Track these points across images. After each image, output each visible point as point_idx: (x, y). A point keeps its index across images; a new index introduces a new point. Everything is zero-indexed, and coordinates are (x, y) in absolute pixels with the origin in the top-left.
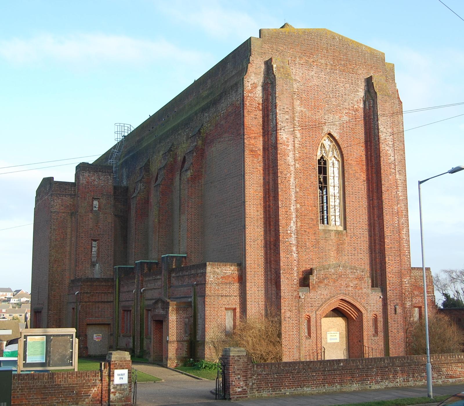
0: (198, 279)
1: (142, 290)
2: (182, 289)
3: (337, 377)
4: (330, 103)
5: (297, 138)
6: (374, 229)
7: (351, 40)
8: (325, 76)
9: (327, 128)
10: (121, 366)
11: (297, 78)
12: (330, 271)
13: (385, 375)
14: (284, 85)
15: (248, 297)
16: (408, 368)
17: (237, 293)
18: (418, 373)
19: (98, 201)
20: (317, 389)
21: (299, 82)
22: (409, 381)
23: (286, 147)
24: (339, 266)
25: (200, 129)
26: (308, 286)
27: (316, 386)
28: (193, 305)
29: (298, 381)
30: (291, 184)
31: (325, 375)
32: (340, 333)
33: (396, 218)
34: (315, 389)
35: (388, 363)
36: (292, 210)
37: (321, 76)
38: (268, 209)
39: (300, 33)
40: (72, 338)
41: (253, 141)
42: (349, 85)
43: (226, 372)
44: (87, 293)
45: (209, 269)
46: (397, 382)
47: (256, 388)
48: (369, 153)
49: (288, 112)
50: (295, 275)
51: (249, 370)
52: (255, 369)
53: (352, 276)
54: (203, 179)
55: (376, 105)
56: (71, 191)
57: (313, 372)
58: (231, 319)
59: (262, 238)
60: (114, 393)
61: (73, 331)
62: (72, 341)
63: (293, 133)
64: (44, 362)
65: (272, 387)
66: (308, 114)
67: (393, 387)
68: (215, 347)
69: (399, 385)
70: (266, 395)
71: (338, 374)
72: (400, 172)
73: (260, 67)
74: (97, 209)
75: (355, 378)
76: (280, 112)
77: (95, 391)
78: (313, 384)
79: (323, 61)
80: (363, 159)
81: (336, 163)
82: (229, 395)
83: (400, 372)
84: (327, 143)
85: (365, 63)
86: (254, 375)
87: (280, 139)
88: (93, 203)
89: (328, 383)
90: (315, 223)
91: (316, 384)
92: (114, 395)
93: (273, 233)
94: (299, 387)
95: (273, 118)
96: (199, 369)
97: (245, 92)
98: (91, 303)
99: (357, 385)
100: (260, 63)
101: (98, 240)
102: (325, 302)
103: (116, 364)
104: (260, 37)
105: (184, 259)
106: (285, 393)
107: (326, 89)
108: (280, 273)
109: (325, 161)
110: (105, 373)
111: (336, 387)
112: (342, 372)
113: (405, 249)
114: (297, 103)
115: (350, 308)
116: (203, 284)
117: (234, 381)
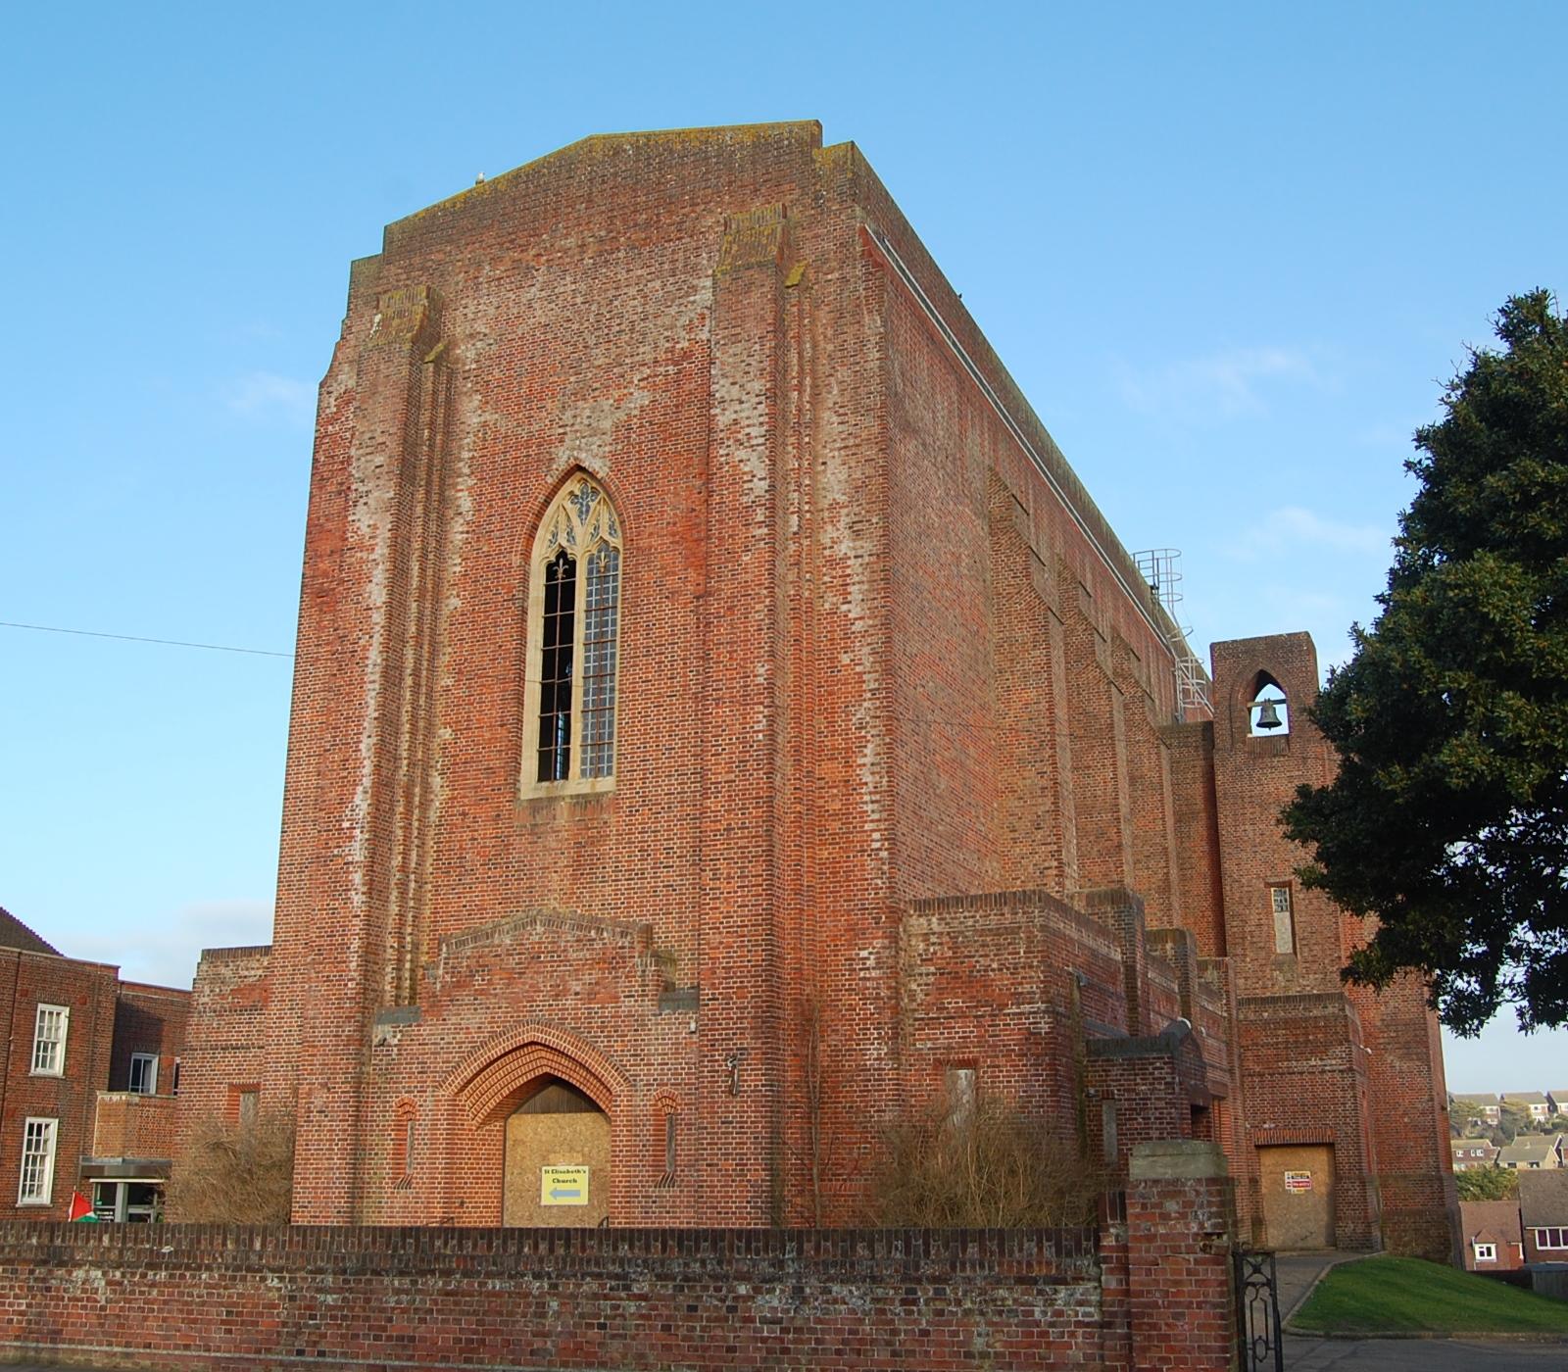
5: (460, 514)
8: (573, 287)
9: (568, 452)
12: (496, 942)
21: (485, 335)
23: (364, 555)
24: (534, 922)
32: (593, 1174)
36: (364, 750)
42: (659, 282)
49: (384, 443)
66: (505, 426)
76: (361, 451)
79: (571, 242)
80: (698, 521)
90: (499, 781)
113: (867, 827)
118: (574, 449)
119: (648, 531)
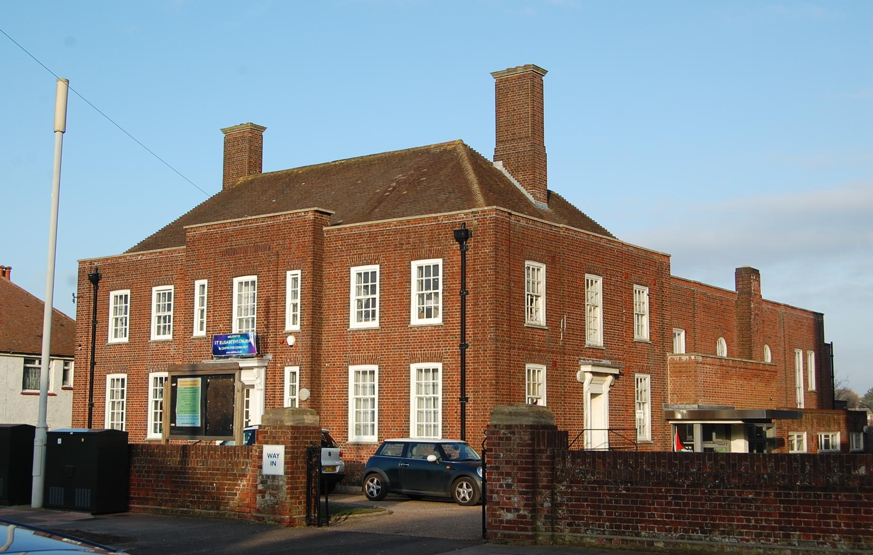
3: (835, 511)
10: (274, 438)
20: (759, 544)
27: (758, 535)
29: (694, 511)
31: (789, 502)
34: (752, 542)
47: (567, 518)
52: (569, 465)
57: (744, 487)
65: (611, 521)
70: (593, 541)
71: (842, 504)
77: (244, 486)
78: (743, 527)
86: (560, 482)
92: (263, 497)
106: (651, 544)
111: (834, 546)
112: (860, 497)
117: (497, 493)
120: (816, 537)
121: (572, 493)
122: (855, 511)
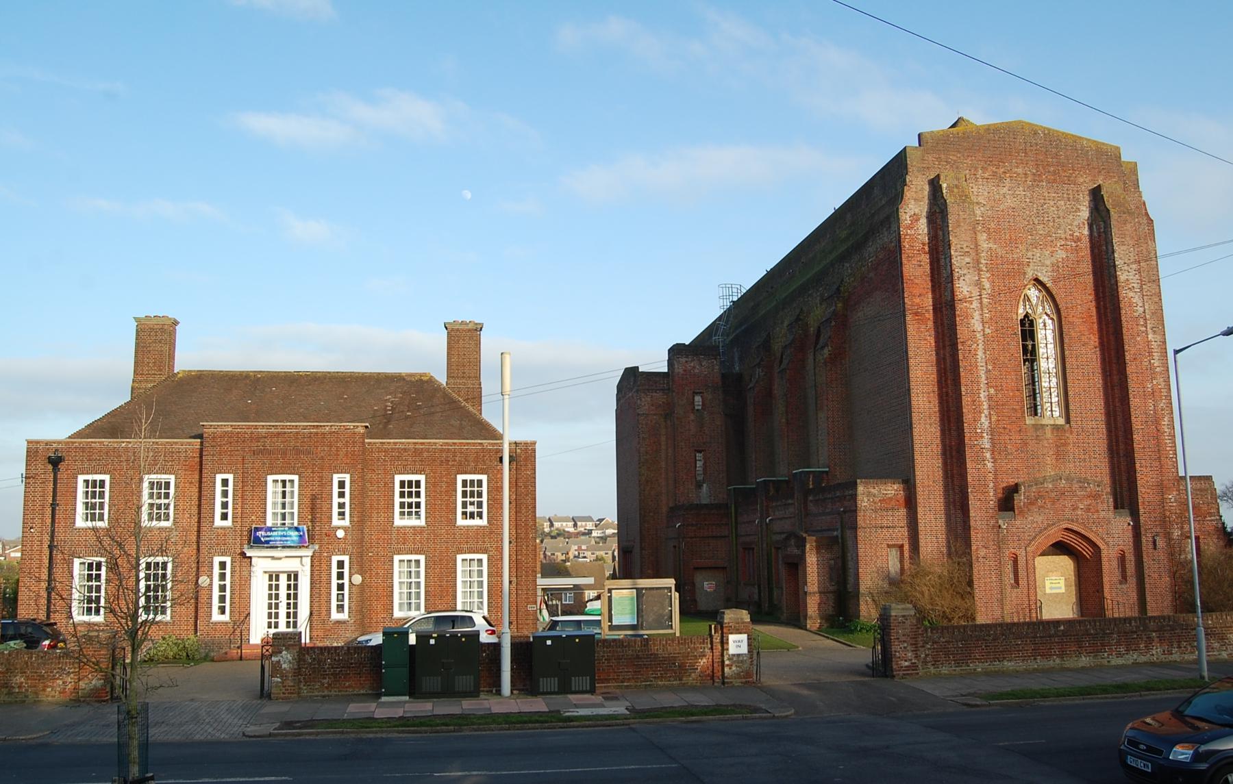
0: (846, 503)
1: (768, 520)
2: (824, 517)
4: (1034, 232)
5: (985, 289)
6: (1115, 420)
7: (1063, 133)
8: (1024, 193)
10: (738, 630)
11: (981, 200)
12: (1046, 486)
13: (1133, 644)
14: (961, 213)
15: (921, 527)
16: (1171, 634)
17: (904, 523)
18: (1187, 641)
19: (701, 396)
22: (1172, 654)
23: (967, 305)
24: (1061, 479)
25: (840, 286)
26: (1012, 509)
27: (1023, 660)
28: (840, 541)
30: (979, 360)
31: (1036, 644)
32: (1066, 579)
33: (1151, 401)
35: (1136, 627)
36: (983, 398)
37: (1019, 193)
38: (945, 398)
39: (982, 132)
40: (671, 592)
41: (917, 300)
43: (886, 639)
44: (692, 525)
45: (860, 489)
46: (1153, 655)
48: (1102, 303)
49: (968, 252)
50: (991, 494)
51: (920, 636)
52: (929, 634)
53: (1082, 493)
54: (847, 359)
55: (1109, 230)
56: (664, 384)
57: (1017, 639)
58: (896, 560)
59: (938, 441)
60: (730, 666)
61: (670, 582)
62: (671, 596)
63: (978, 284)
64: (636, 623)
65: (954, 660)
66: (1001, 252)
67: (1145, 663)
68: (874, 600)
69: (1155, 659)
71: (1056, 643)
72: (1154, 329)
73: (922, 189)
74: (700, 408)
75: (1084, 649)
76: (957, 253)
78: (1019, 657)
79: (1020, 170)
81: (1049, 322)
82: (892, 671)
83: (1156, 640)
84: (1033, 293)
85: (1088, 165)
86: (927, 643)
87: (958, 294)
88: (694, 400)
89: (1041, 656)
90: (1019, 415)
91: (1022, 657)
92: (730, 669)
93: (954, 433)
94: (995, 661)
95: (946, 263)
96: (852, 632)
97: (901, 229)
98: (698, 539)
99: (1088, 658)
100: (922, 183)
101: (703, 451)
102: (1040, 532)
103: (731, 627)
104: (920, 145)
105: (825, 475)
106: (975, 670)
107: (1028, 212)
108: (968, 492)
109: (1032, 321)
110: (717, 639)
111: (1054, 661)
113: (1168, 449)
114: (982, 237)
115: (1080, 541)
116: (853, 511)
117: (899, 652)
118: (1034, 270)
119: (1072, 314)
120: (1047, 658)
121: (934, 649)
122: (1062, 645)
